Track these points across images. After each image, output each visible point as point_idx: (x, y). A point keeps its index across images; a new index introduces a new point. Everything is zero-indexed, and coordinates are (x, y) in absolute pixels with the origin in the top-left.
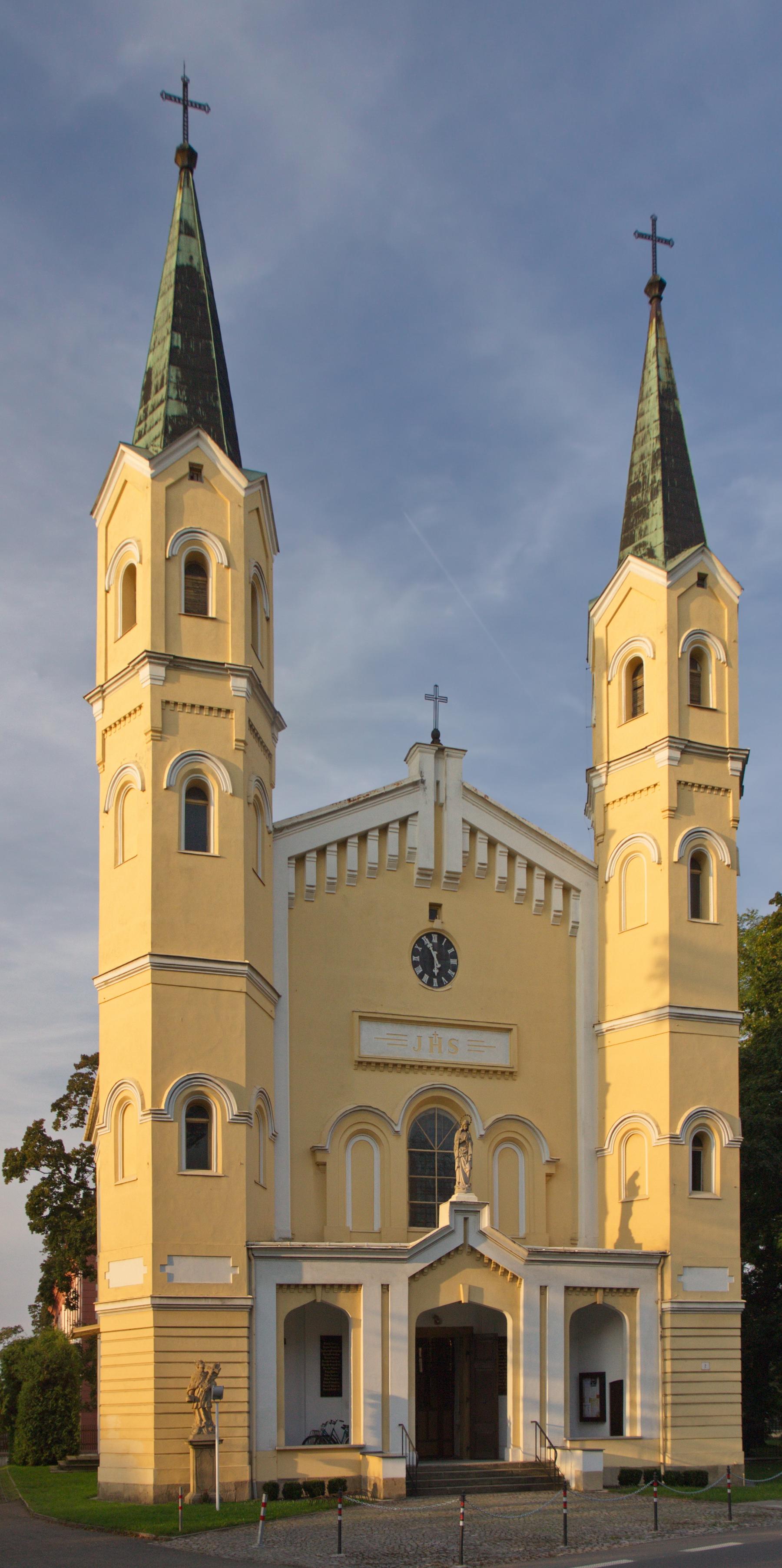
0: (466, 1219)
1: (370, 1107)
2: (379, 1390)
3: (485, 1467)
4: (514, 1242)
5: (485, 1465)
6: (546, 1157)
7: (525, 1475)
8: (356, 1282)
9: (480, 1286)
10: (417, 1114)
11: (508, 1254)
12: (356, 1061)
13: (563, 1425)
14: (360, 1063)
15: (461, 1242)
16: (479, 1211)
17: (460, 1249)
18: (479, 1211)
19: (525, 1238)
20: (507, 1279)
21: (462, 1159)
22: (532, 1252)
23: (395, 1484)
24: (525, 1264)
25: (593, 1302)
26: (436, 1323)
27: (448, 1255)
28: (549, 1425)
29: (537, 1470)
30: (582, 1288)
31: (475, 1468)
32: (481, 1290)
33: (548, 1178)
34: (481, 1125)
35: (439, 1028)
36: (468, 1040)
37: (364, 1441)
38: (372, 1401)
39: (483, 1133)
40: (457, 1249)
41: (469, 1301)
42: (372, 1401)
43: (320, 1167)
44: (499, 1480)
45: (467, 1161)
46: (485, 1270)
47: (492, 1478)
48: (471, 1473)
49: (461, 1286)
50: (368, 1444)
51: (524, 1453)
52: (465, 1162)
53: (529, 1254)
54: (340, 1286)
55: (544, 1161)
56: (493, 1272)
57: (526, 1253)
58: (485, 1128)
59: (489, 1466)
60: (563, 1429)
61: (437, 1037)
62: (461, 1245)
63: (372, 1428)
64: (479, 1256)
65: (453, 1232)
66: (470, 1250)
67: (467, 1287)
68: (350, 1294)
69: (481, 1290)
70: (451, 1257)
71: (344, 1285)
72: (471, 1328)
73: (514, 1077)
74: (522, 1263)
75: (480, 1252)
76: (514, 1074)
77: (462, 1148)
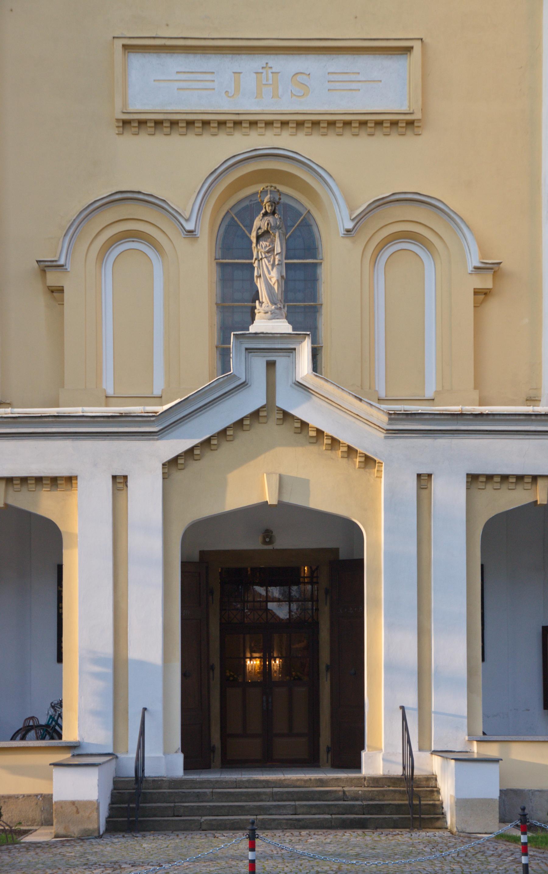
0: (271, 365)
1: (139, 192)
2: (108, 650)
3: (298, 783)
4: (361, 400)
5: (298, 780)
6: (475, 261)
7: (371, 800)
8: (66, 474)
9: (302, 474)
10: (232, 202)
11: (354, 420)
12: (118, 120)
13: (465, 714)
14: (126, 123)
15: (264, 402)
16: (295, 349)
17: (261, 414)
18: (295, 349)
19: (433, 400)
20: (355, 464)
21: (265, 261)
22: (394, 416)
23: (78, 812)
24: (386, 438)
25: (531, 500)
26: (265, 542)
27: (239, 424)
28: (435, 713)
29: (395, 791)
30: (505, 478)
31: (267, 784)
32: (305, 483)
33: (482, 297)
34: (345, 212)
35: (272, 57)
36: (329, 73)
37: (80, 735)
38: (97, 669)
39: (350, 225)
40: (255, 415)
41: (279, 501)
42: (97, 669)
43: (55, 294)
44: (311, 806)
45: (273, 265)
46: (314, 449)
47: (297, 803)
48: (265, 793)
49: (265, 475)
50: (86, 740)
51: (384, 760)
52: (270, 268)
53: (390, 419)
54: (39, 480)
55: (470, 269)
56: (329, 452)
57: (385, 418)
58: (352, 218)
59: (306, 781)
60: (465, 721)
61: (270, 71)
62: (263, 407)
63: (96, 713)
64: (298, 425)
65: (244, 385)
66: (281, 416)
67: (276, 479)
68: (57, 494)
69: (305, 483)
70: (245, 428)
71: (47, 478)
72: (336, 551)
73: (416, 130)
74: (381, 435)
75: (299, 419)
76: (416, 124)
77: (263, 243)
